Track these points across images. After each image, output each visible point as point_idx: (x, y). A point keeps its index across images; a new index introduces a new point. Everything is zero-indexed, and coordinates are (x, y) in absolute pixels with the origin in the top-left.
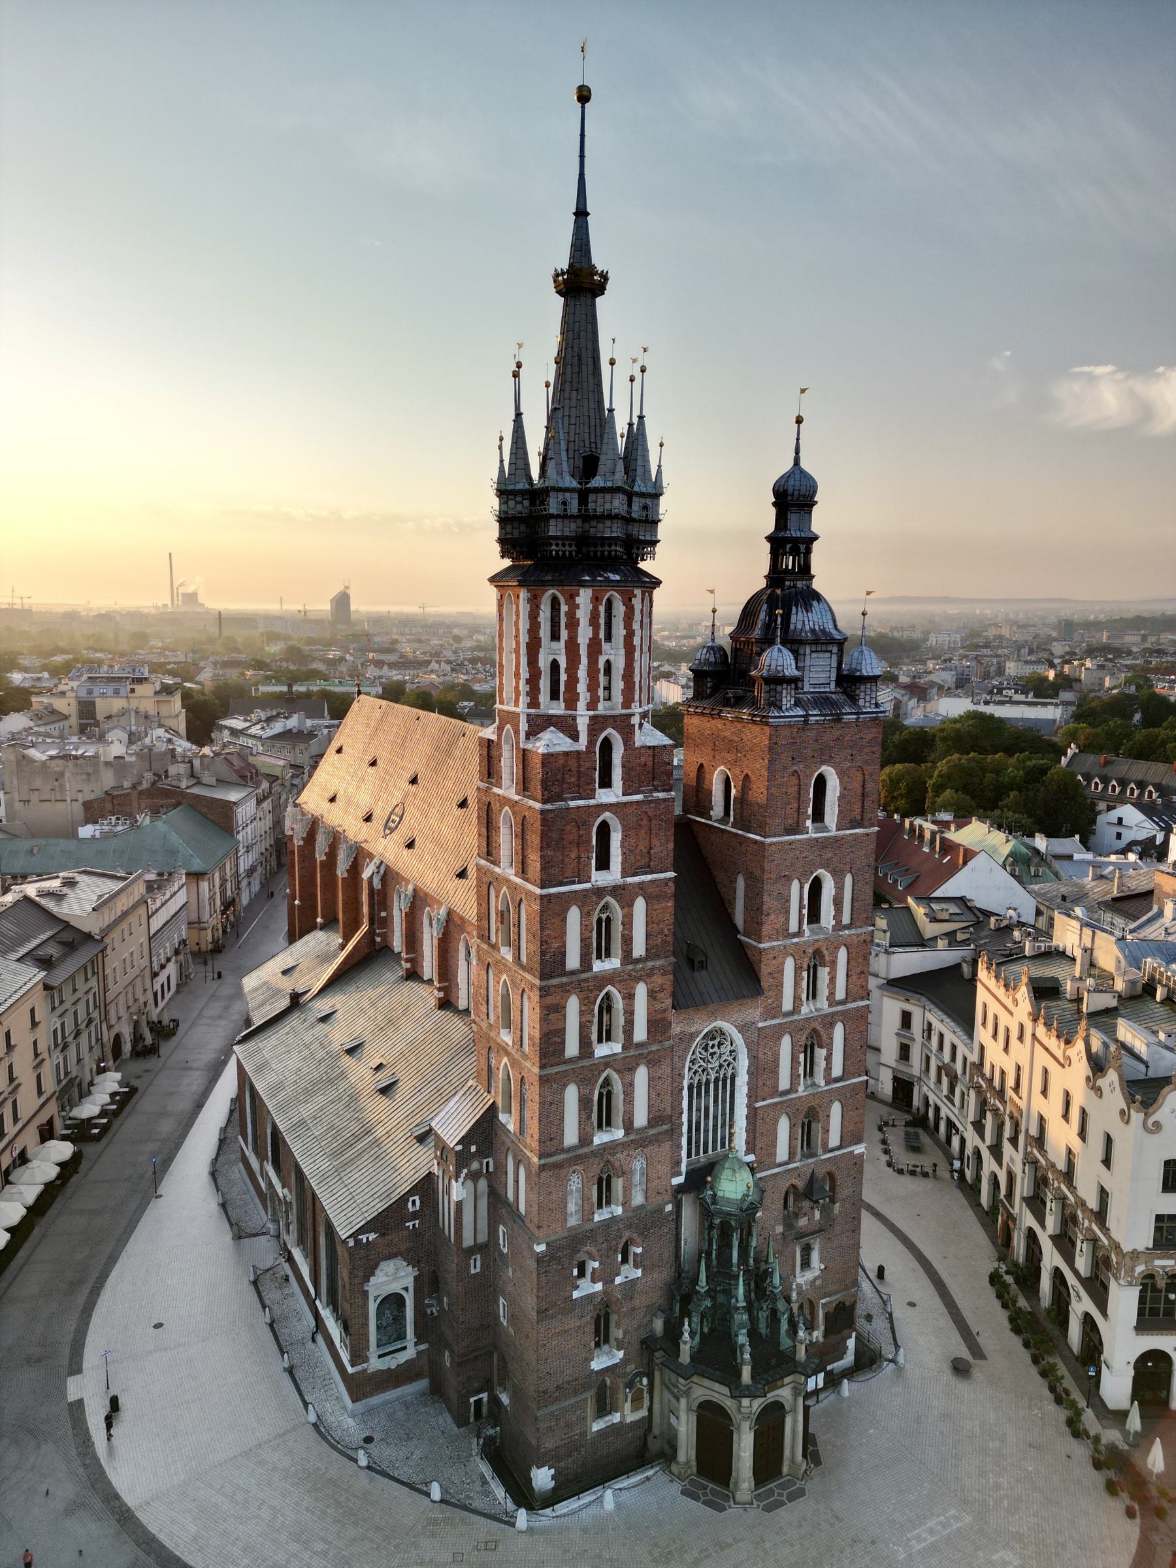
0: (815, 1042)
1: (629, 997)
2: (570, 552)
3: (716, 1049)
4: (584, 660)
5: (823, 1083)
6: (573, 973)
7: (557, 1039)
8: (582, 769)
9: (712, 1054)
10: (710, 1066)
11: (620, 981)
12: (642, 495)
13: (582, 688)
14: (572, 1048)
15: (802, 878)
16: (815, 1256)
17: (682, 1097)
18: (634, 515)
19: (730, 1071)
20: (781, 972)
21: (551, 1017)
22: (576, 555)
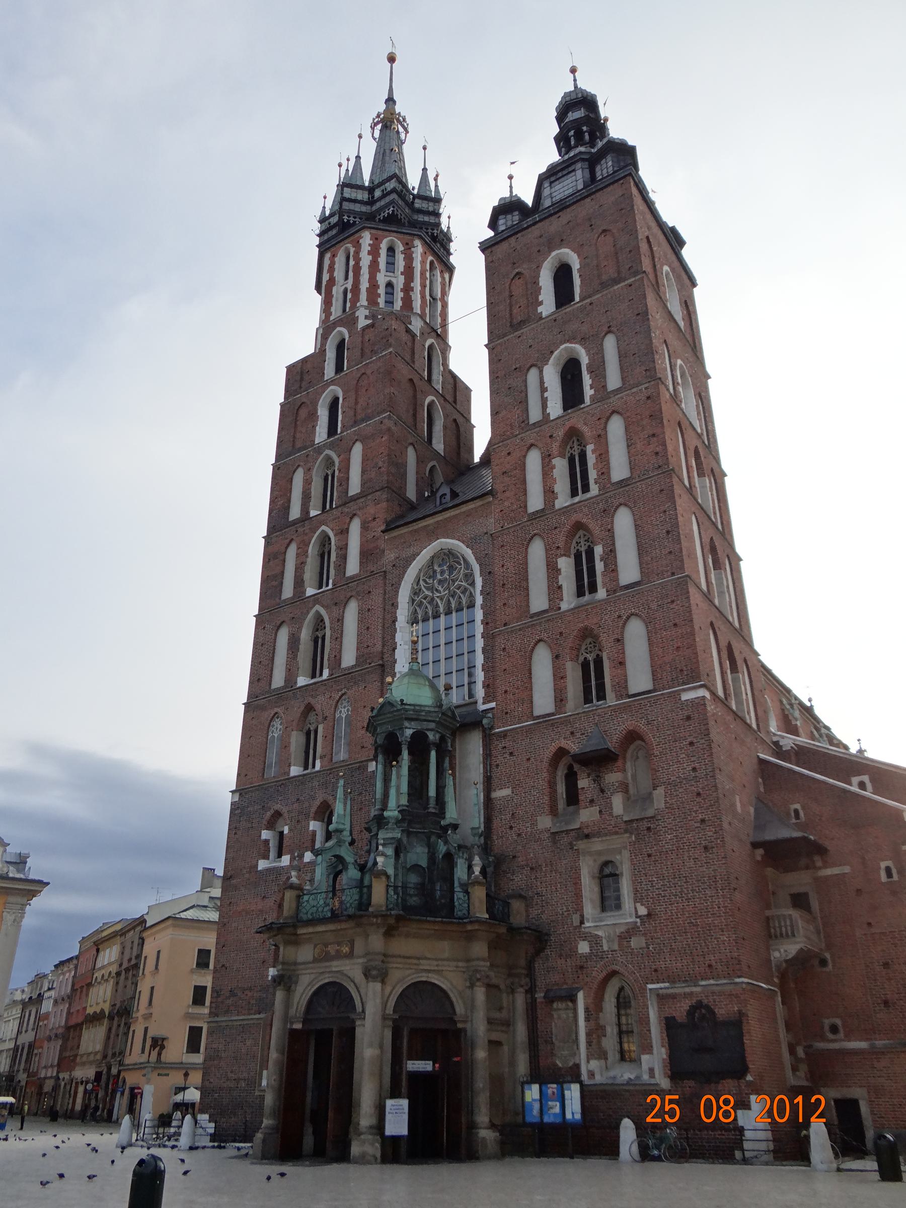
0: (592, 546)
1: (344, 532)
3: (446, 575)
7: (274, 583)
9: (440, 582)
11: (333, 520)
14: (288, 591)
15: (539, 364)
16: (626, 886)
17: (395, 630)
19: (464, 601)
20: (522, 467)
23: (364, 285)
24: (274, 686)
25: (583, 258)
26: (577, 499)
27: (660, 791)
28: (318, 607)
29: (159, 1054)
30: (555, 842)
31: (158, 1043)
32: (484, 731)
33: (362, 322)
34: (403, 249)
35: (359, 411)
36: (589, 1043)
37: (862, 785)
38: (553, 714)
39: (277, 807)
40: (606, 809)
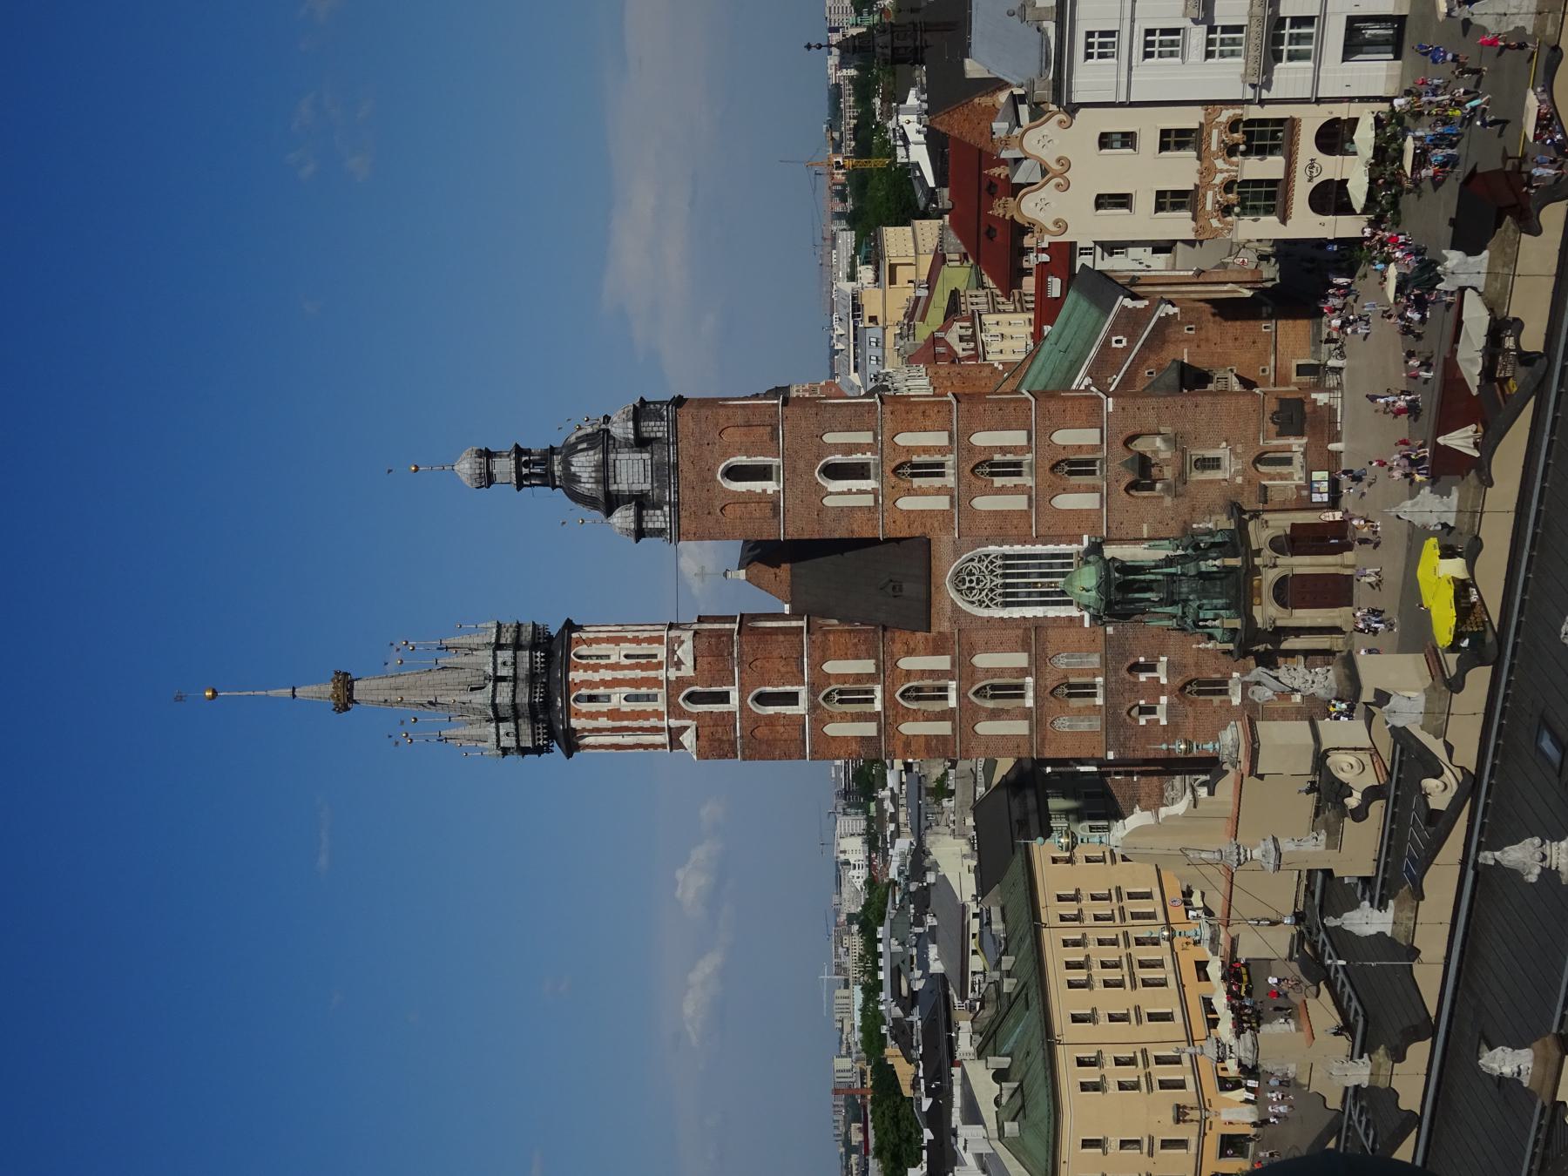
2: (544, 728)
3: (974, 578)
4: (625, 723)
5: (1029, 456)
6: (879, 730)
8: (711, 724)
9: (978, 584)
10: (988, 586)
11: (893, 685)
12: (495, 669)
13: (646, 724)
14: (944, 728)
16: (1210, 454)
18: (511, 673)
21: (913, 748)
22: (543, 721)
23: (639, 674)
24: (1026, 732)
25: (739, 452)
26: (950, 471)
27: (1162, 430)
28: (970, 694)
29: (1192, 1108)
30: (1181, 495)
31: (1180, 1114)
32: (1103, 542)
33: (688, 670)
34: (585, 646)
35: (789, 669)
36: (1286, 479)
37: (1117, 342)
38: (1102, 495)
39: (1124, 712)
40: (1167, 462)
